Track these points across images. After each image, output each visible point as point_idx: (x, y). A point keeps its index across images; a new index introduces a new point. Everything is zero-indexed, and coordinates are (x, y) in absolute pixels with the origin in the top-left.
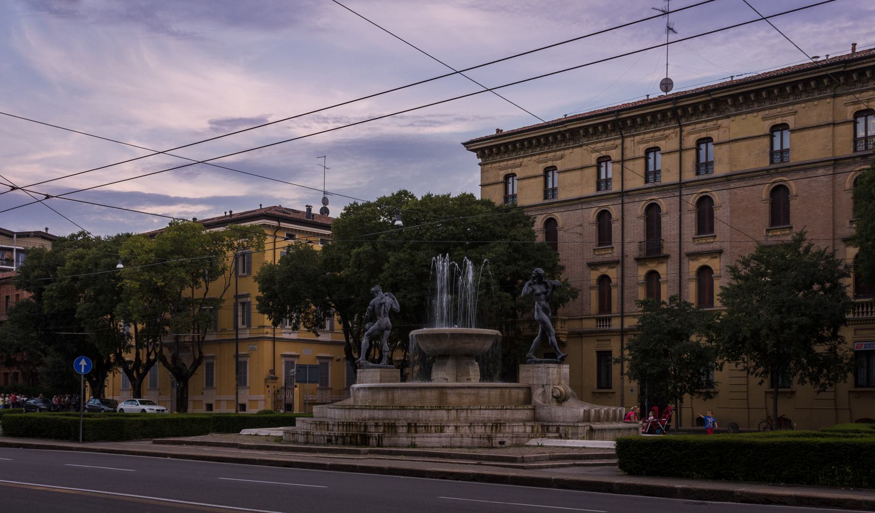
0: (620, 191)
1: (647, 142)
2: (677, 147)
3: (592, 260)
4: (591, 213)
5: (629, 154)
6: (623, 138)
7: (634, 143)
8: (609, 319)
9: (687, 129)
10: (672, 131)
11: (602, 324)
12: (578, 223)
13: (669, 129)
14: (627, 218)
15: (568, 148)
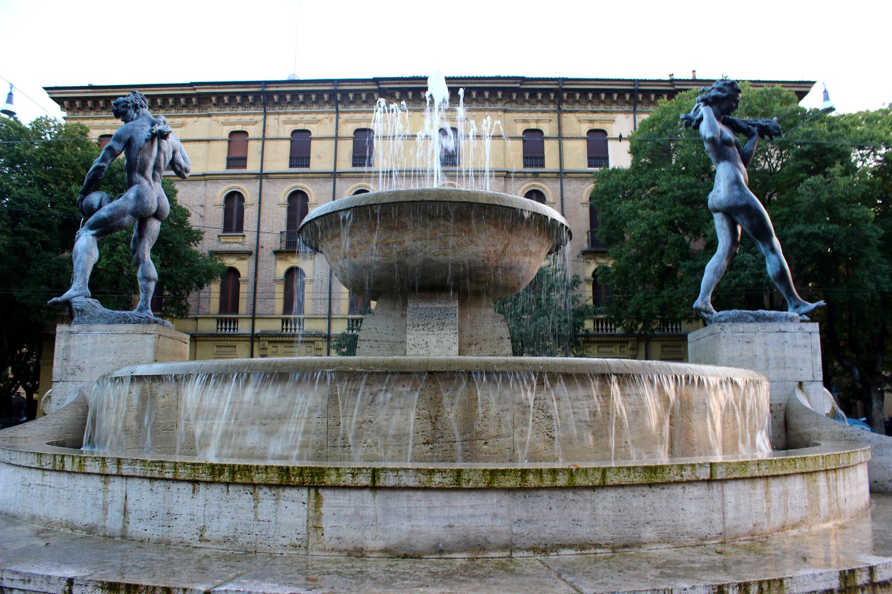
0: (259, 172)
1: (296, 123)
2: (334, 134)
3: (215, 249)
4: (220, 191)
5: (270, 133)
6: (265, 114)
8: (235, 321)
9: (343, 117)
10: (326, 115)
11: (232, 327)
12: (199, 203)
13: (323, 113)
15: (192, 116)
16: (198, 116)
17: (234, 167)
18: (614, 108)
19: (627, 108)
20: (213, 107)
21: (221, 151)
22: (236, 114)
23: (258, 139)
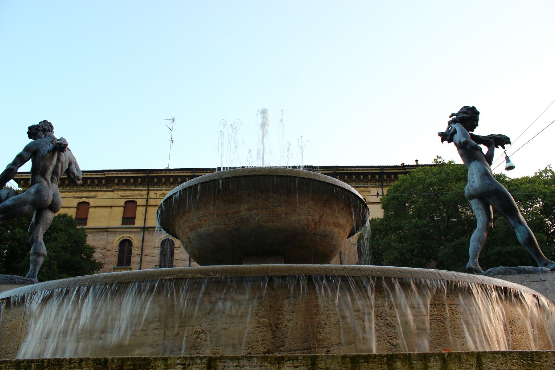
4: (116, 239)
5: (151, 202)
6: (149, 190)
7: (157, 195)
14: (145, 247)
15: (102, 191)
16: (106, 191)
17: (127, 224)
18: (369, 184)
19: (377, 184)
20: (115, 186)
21: (119, 212)
22: (130, 190)
23: (143, 206)
